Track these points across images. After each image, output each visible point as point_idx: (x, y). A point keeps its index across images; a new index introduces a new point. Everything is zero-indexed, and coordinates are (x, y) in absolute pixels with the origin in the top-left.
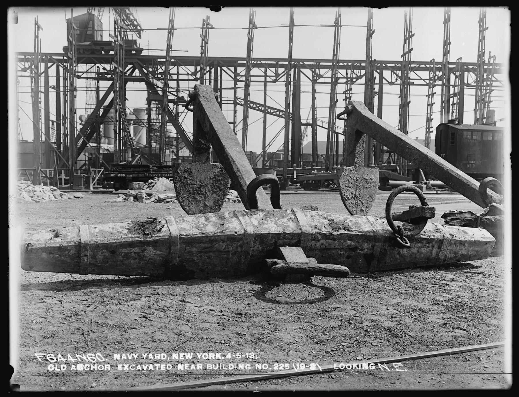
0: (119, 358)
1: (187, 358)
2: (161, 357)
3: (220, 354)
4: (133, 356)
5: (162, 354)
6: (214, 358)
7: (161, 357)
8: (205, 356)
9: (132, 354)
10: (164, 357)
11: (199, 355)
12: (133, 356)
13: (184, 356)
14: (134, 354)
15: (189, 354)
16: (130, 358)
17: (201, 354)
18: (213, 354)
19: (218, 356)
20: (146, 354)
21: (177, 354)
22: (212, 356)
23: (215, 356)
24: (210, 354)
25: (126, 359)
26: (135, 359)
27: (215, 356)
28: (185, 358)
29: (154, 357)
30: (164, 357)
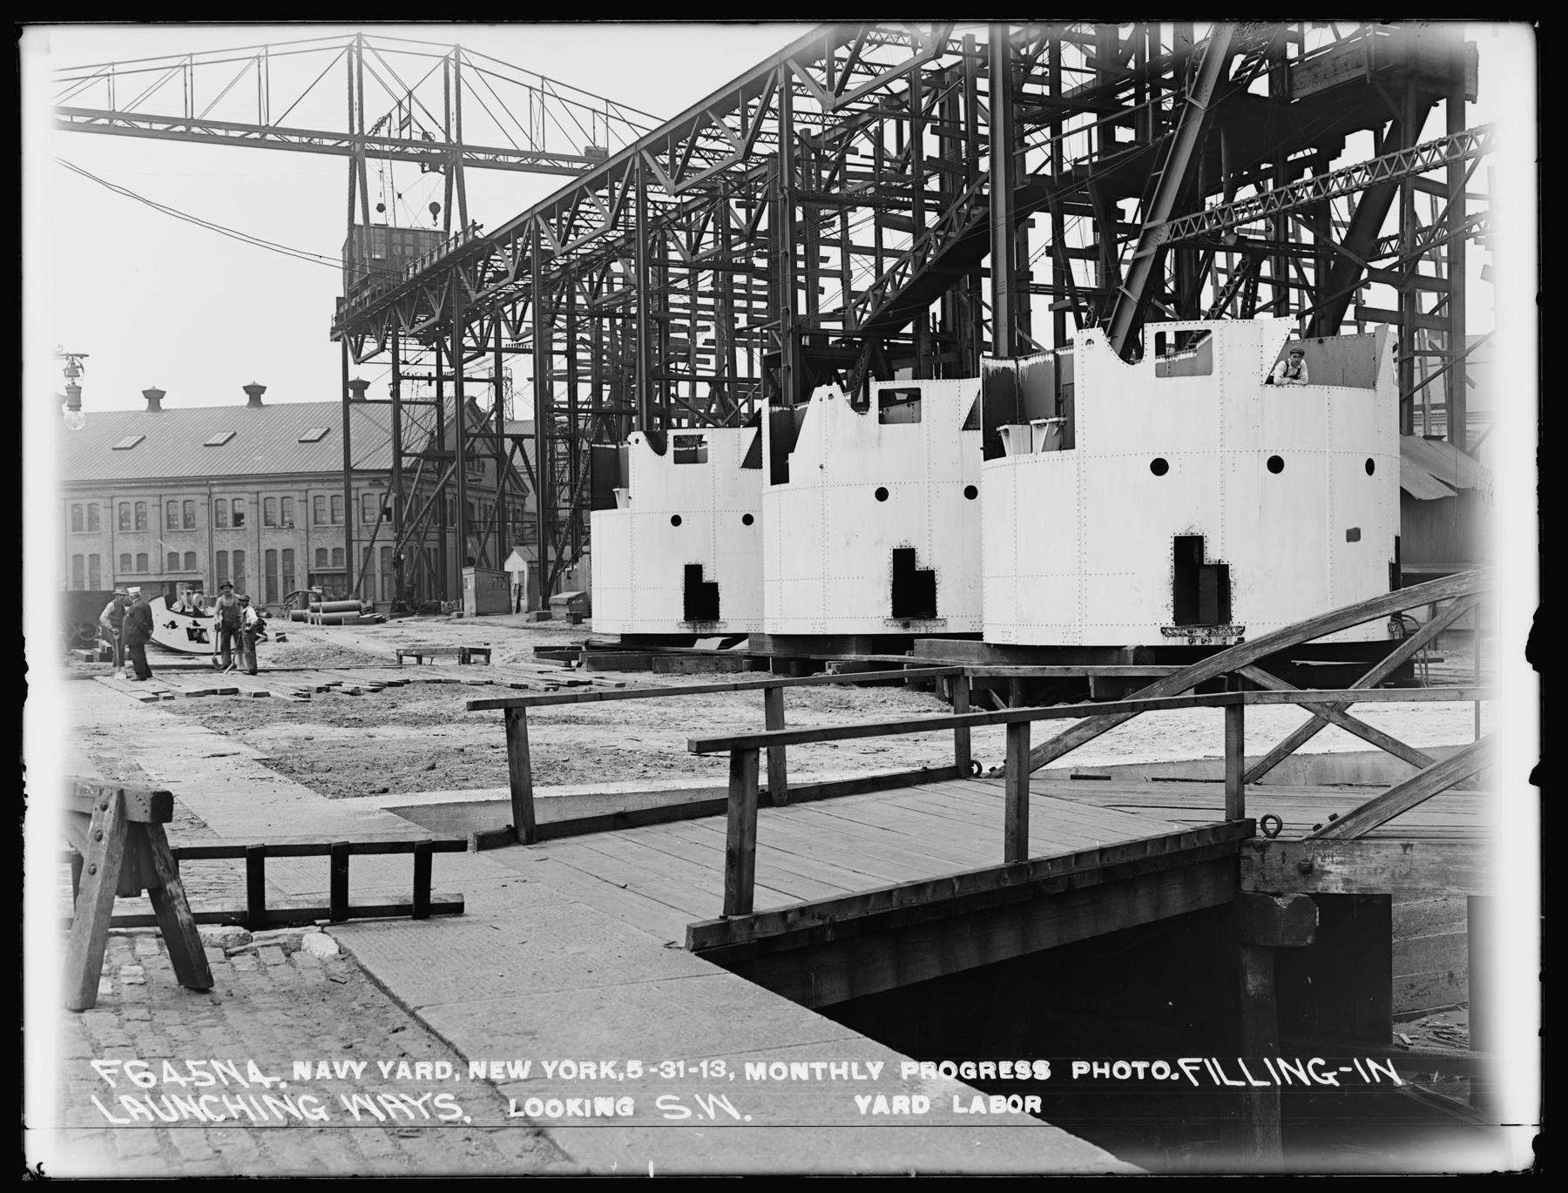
0: (307, 1077)
1: (513, 1076)
2: (434, 1072)
3: (612, 1064)
4: (350, 1068)
5: (439, 1065)
6: (593, 1077)
7: (434, 1072)
8: (568, 1071)
9: (347, 1064)
10: (444, 1071)
11: (549, 1071)
12: (350, 1068)
13: (505, 1067)
14: (353, 1064)
15: (518, 1063)
16: (342, 1075)
17: (554, 1064)
18: (593, 1066)
19: (607, 1069)
20: (391, 1064)
21: (484, 1064)
22: (587, 1071)
23: (598, 1071)
24: (582, 1065)
25: (329, 1077)
26: (358, 1076)
27: (598, 1071)
28: (508, 1076)
29: (413, 1072)
30: (444, 1071)
